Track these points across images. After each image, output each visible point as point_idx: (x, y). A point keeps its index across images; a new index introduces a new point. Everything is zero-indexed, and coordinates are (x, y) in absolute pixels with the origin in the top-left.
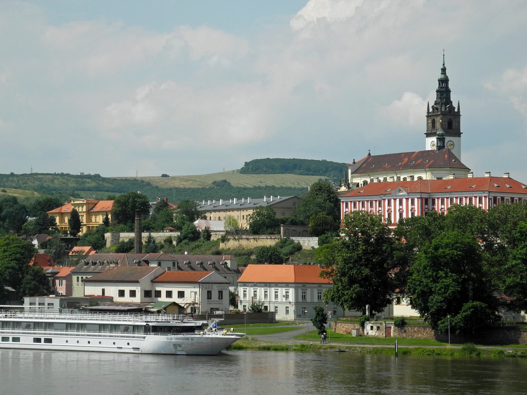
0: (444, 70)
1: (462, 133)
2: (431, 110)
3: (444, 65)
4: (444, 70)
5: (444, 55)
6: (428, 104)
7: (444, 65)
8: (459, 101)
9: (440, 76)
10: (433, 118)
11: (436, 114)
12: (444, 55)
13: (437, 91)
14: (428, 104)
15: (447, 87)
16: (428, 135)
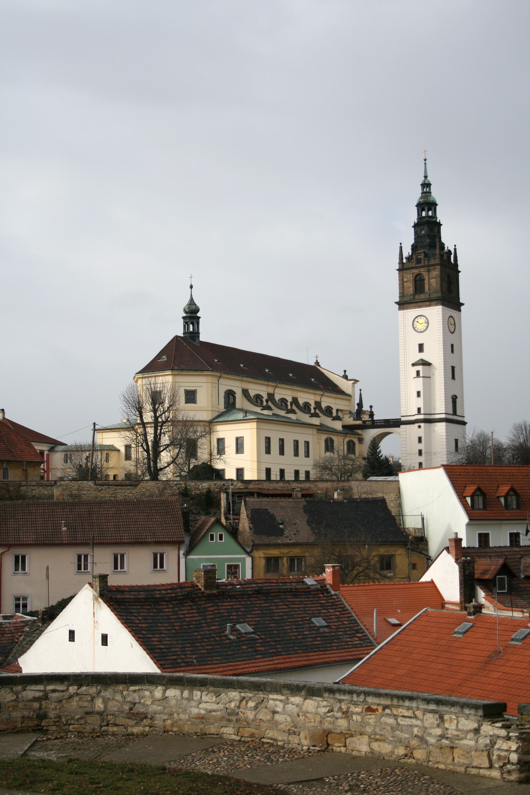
0: (426, 185)
1: (463, 304)
2: (405, 261)
3: (426, 177)
4: (426, 185)
5: (425, 160)
6: (401, 247)
7: (426, 177)
8: (455, 246)
9: (417, 195)
10: (416, 271)
11: (426, 263)
12: (425, 160)
13: (415, 226)
14: (401, 247)
15: (435, 216)
16: (403, 304)
